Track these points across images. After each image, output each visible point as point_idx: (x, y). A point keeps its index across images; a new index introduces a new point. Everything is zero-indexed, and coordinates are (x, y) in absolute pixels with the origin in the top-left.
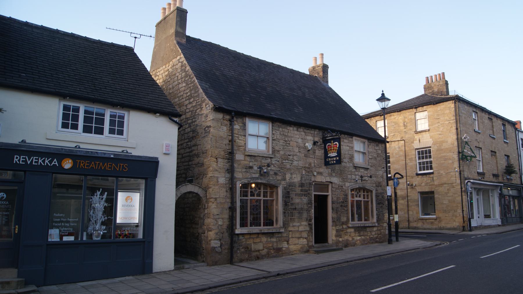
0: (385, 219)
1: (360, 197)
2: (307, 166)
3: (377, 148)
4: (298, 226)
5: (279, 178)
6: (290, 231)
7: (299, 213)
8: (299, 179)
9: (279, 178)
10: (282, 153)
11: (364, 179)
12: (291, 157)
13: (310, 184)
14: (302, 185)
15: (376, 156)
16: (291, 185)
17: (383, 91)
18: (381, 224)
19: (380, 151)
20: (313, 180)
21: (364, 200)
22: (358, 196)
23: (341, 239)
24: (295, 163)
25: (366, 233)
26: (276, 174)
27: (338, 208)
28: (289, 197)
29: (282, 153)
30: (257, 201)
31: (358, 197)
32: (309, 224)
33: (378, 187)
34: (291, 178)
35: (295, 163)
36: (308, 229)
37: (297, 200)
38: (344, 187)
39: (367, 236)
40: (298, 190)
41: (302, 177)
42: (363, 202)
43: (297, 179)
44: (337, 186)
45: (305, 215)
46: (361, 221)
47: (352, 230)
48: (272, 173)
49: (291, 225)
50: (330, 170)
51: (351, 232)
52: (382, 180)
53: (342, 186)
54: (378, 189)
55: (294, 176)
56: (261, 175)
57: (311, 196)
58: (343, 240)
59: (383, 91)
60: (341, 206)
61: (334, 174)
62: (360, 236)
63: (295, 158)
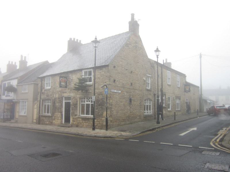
0: (104, 115)
1: (89, 102)
2: (61, 90)
3: (101, 71)
4: (58, 115)
5: (52, 96)
6: (55, 116)
7: (58, 110)
8: (58, 95)
9: (52, 96)
10: (53, 87)
11: (88, 92)
12: (56, 88)
13: (62, 97)
14: (59, 98)
15: (100, 76)
16: (55, 99)
17: (96, 36)
18: (101, 118)
19: (104, 73)
20: (63, 95)
21: (92, 103)
22: (88, 101)
23: (75, 123)
24: (57, 90)
25: (89, 122)
26: (51, 95)
27: (73, 107)
28: (55, 103)
29: (53, 87)
30: (49, 105)
31: (88, 101)
32: (61, 114)
33: (100, 95)
34: (56, 96)
35: (57, 90)
36: (61, 116)
37: (57, 105)
38: (76, 97)
39: (90, 123)
40: (58, 100)
41: (59, 95)
42: (90, 105)
43: (57, 96)
44: (73, 97)
45: (59, 110)
46: (49, 113)
47: (81, 119)
48: (50, 95)
49: (55, 114)
50: (70, 90)
51: (79, 120)
52: (103, 91)
53: (75, 97)
54: (99, 97)
55: (56, 95)
56: (47, 96)
57: (62, 102)
58: (75, 124)
59: (96, 36)
60: (75, 107)
61: (71, 92)
62: (86, 123)
63: (57, 88)
